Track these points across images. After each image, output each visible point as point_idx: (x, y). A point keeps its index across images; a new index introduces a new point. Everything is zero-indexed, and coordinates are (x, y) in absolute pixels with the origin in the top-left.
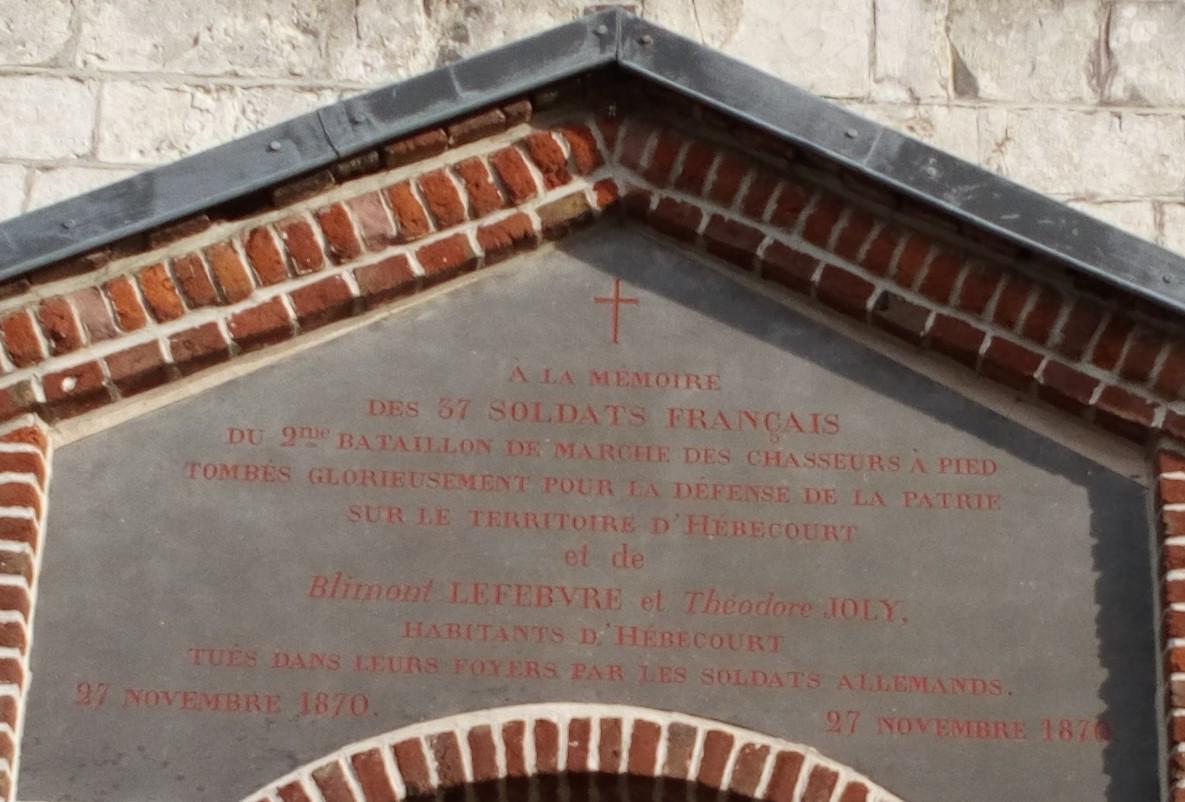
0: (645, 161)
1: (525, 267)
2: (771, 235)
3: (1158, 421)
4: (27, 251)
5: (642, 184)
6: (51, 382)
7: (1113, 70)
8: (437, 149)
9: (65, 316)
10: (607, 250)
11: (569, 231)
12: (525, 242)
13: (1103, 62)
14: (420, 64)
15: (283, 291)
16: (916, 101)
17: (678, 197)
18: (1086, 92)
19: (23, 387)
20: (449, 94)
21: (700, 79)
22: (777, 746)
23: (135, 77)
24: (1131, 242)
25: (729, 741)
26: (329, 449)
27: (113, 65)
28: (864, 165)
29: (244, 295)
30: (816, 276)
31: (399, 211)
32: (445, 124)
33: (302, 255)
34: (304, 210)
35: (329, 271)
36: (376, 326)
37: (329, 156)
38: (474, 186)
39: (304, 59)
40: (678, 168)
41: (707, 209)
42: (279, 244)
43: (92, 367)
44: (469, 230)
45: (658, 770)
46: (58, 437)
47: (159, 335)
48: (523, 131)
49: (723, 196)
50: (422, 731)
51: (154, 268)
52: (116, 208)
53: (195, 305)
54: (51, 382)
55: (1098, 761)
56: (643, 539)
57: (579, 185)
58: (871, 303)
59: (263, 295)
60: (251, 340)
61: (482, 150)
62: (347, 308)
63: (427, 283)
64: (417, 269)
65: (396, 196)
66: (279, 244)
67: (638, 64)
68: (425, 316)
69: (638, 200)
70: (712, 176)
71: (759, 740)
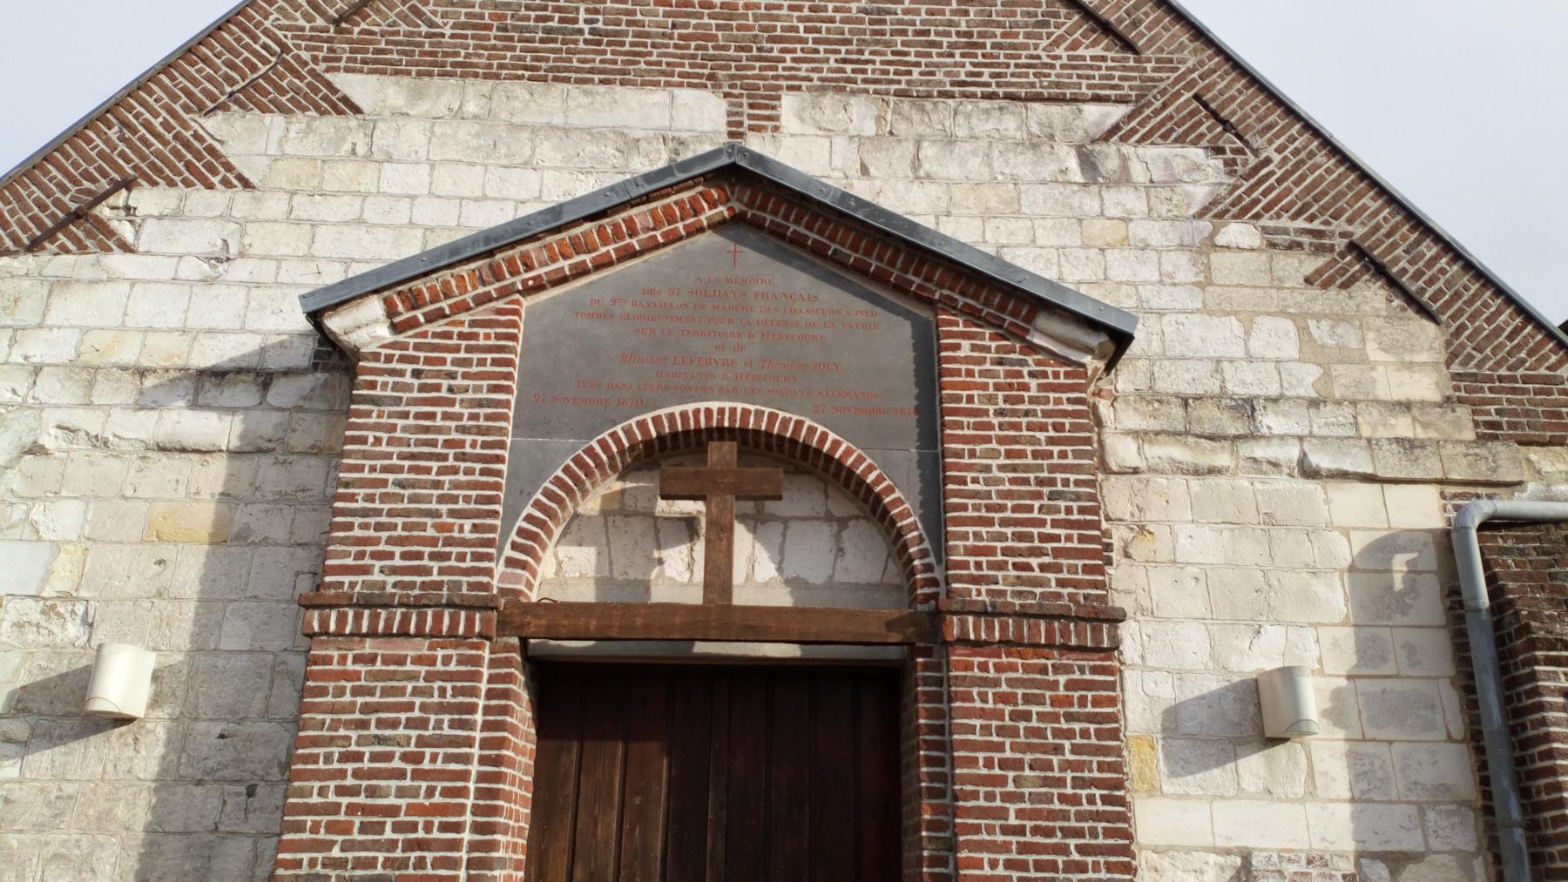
0: (746, 200)
1: (702, 239)
2: (793, 227)
3: (937, 296)
4: (515, 234)
5: (744, 208)
6: (524, 282)
7: (920, 166)
8: (668, 195)
9: (530, 257)
10: (731, 233)
11: (718, 226)
12: (701, 230)
13: (916, 163)
14: (662, 164)
15: (611, 248)
16: (847, 177)
18: (910, 174)
19: (514, 284)
20: (673, 175)
21: (766, 168)
22: (795, 417)
23: (556, 168)
24: (927, 230)
25: (777, 416)
26: (628, 307)
27: (547, 164)
28: (827, 201)
29: (596, 249)
30: (809, 243)
31: (654, 219)
32: (671, 186)
33: (618, 235)
34: (619, 218)
35: (628, 240)
36: (645, 261)
37: (628, 198)
38: (682, 209)
39: (619, 162)
40: (758, 202)
41: (769, 218)
42: (609, 231)
43: (540, 276)
44: (680, 225)
45: (751, 427)
46: (527, 302)
47: (565, 265)
48: (700, 188)
49: (775, 212)
50: (663, 412)
51: (563, 239)
52: (549, 217)
53: (578, 253)
54: (524, 282)
55: (914, 423)
56: (745, 340)
57: (721, 208)
58: (830, 253)
59: (603, 250)
60: (599, 267)
61: (685, 195)
62: (634, 254)
63: (665, 245)
64: (661, 240)
65: (653, 212)
66: (609, 231)
67: (743, 163)
68: (663, 258)
70: (770, 205)
71: (788, 415)
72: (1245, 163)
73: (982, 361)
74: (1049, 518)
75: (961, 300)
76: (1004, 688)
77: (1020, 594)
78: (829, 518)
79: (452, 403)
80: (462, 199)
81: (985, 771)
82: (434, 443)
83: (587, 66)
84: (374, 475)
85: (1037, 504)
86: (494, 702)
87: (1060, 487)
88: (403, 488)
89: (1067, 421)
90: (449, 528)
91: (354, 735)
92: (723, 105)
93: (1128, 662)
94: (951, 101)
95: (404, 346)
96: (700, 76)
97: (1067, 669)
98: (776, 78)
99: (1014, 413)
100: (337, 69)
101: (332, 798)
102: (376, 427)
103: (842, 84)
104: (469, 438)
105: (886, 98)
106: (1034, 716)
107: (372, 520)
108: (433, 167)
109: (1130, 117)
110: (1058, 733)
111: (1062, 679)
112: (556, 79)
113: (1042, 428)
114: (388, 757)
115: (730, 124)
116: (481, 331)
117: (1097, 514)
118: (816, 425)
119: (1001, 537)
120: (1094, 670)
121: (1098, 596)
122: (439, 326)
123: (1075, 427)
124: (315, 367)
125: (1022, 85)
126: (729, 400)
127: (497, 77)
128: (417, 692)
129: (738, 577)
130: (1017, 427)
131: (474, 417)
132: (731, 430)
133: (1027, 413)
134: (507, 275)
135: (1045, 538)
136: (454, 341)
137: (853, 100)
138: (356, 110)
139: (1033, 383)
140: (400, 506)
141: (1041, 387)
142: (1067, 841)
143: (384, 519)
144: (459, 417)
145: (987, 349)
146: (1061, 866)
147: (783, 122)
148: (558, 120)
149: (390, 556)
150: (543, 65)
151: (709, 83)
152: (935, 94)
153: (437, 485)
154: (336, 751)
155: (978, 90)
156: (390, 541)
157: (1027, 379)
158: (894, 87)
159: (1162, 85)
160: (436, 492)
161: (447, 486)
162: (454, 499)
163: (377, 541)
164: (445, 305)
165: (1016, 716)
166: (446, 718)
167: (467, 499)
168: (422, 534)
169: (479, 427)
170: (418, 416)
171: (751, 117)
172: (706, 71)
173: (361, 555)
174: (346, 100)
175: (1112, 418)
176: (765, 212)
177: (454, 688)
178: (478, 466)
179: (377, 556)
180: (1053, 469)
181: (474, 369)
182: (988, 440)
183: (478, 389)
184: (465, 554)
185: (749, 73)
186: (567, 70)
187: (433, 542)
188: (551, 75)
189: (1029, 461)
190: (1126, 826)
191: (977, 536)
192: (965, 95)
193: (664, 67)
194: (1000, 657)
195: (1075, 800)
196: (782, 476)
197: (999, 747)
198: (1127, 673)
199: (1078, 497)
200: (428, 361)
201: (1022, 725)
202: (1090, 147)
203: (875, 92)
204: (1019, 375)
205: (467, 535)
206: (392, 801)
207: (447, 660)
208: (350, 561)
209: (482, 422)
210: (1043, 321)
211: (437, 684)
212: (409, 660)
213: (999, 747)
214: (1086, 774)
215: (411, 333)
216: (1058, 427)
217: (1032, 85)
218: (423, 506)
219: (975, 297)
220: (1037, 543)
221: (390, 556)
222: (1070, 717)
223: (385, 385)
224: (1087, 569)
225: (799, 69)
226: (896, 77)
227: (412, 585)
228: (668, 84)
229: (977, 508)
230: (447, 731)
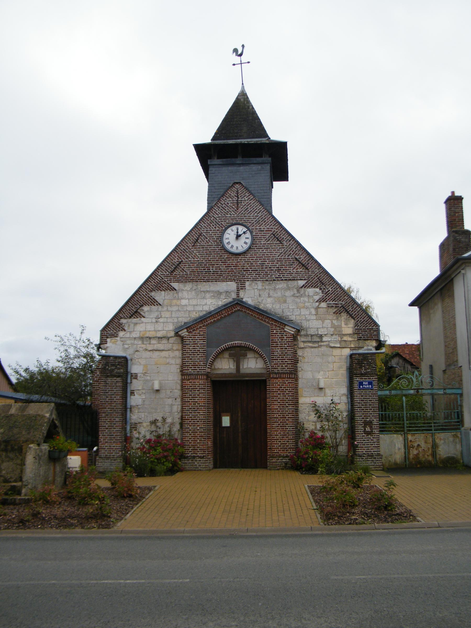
50: (228, 344)
69: (239, 310)
72: (325, 291)
73: (277, 334)
75: (274, 324)
77: (281, 370)
79: (197, 344)
82: (196, 351)
90: (199, 363)
91: (190, 392)
95: (190, 335)
97: (288, 381)
98: (245, 279)
99: (282, 342)
100: (171, 282)
101: (189, 400)
102: (187, 348)
108: (189, 299)
109: (306, 283)
110: (286, 390)
112: (207, 281)
113: (286, 344)
114: (195, 395)
120: (291, 381)
123: (291, 344)
128: (198, 386)
129: (241, 367)
130: (282, 344)
131: (201, 346)
133: (284, 342)
135: (285, 362)
137: (258, 282)
138: (176, 290)
139: (285, 337)
144: (198, 346)
145: (278, 331)
147: (246, 287)
148: (208, 290)
153: (197, 357)
154: (188, 394)
156: (191, 365)
158: (265, 279)
159: (312, 276)
162: (199, 359)
163: (190, 366)
165: (280, 387)
167: (201, 359)
170: (193, 346)
171: (241, 287)
172: (233, 278)
173: (188, 368)
174: (173, 288)
180: (287, 351)
182: (278, 346)
183: (201, 342)
187: (197, 365)
191: (276, 362)
192: (277, 280)
195: (287, 398)
205: (202, 364)
206: (196, 401)
207: (201, 382)
208: (186, 369)
210: (286, 327)
213: (278, 392)
216: (289, 344)
217: (289, 277)
221: (192, 368)
222: (288, 387)
227: (195, 372)
228: (226, 281)
229: (276, 357)
230: (202, 392)
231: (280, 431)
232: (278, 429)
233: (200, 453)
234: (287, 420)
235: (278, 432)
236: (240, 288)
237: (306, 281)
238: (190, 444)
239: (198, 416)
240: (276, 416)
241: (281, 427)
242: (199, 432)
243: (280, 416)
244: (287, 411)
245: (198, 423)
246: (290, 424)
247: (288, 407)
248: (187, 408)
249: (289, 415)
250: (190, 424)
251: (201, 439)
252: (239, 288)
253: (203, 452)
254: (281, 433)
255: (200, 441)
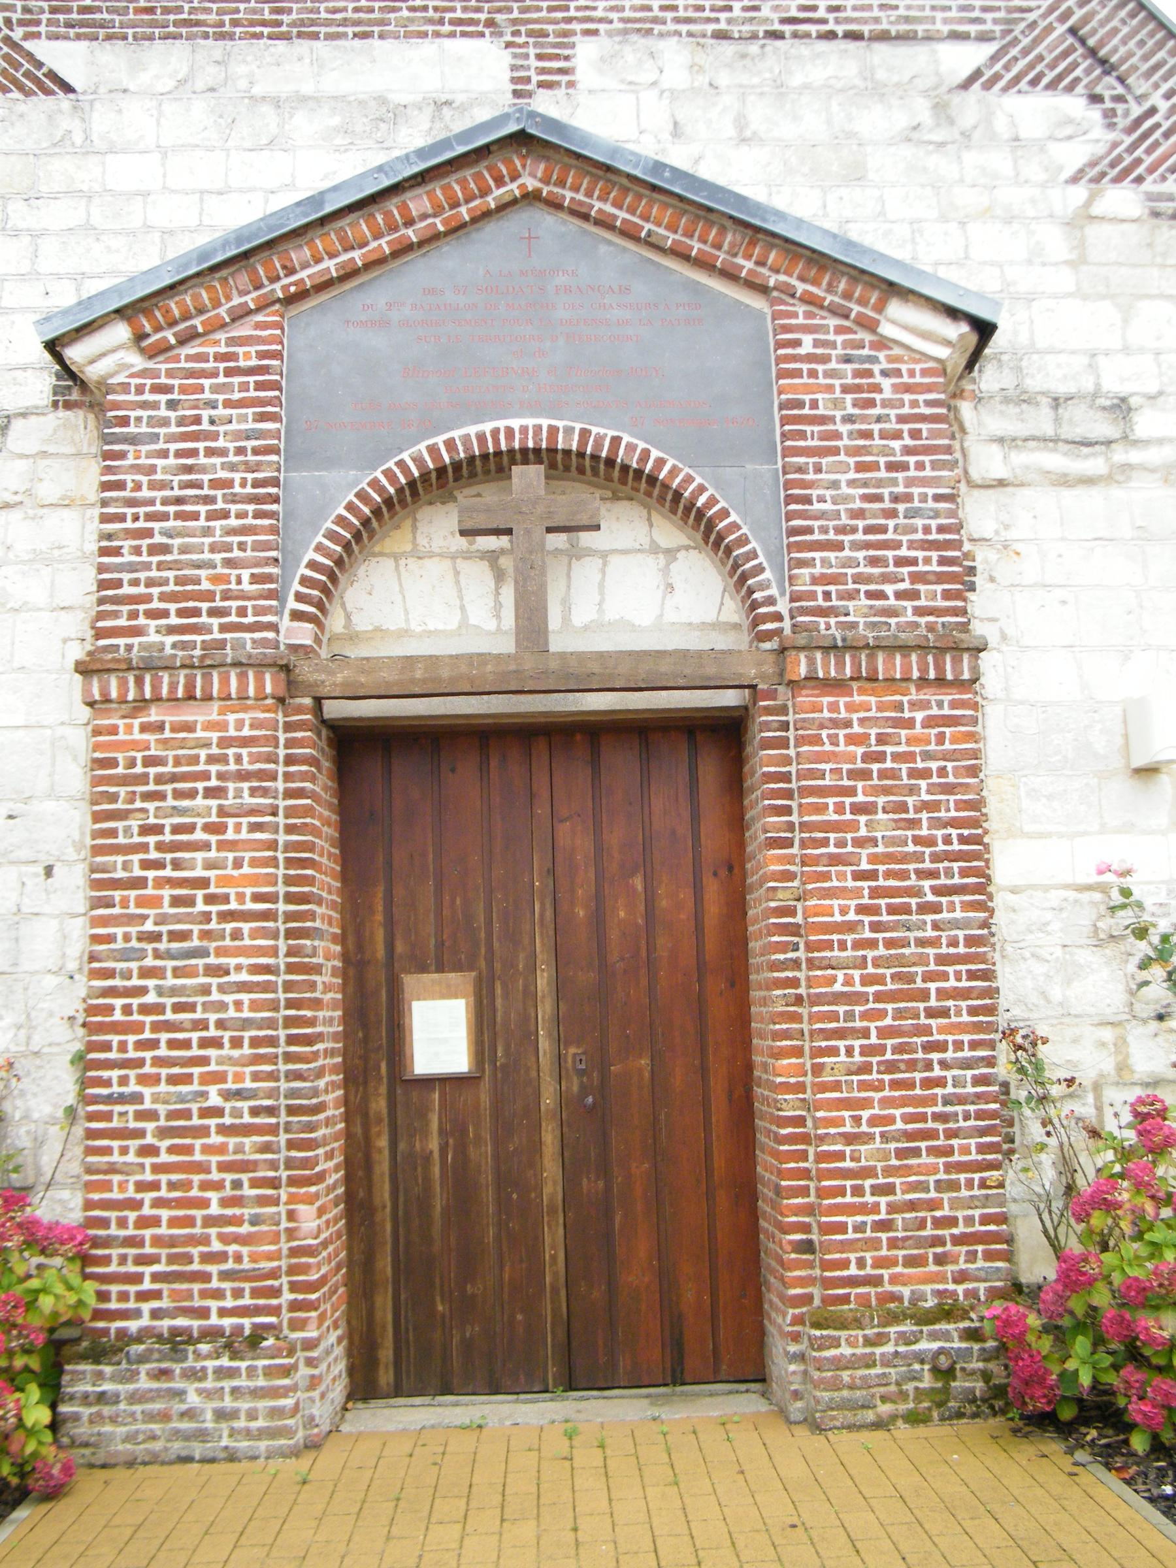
0: (539, 175)
2: (598, 205)
3: (771, 283)
4: (271, 230)
5: (539, 185)
6: (285, 288)
17: (556, 190)
19: (273, 291)
25: (590, 432)
28: (638, 173)
30: (618, 224)
40: (555, 177)
41: (569, 195)
43: (302, 280)
44: (463, 210)
49: (576, 189)
50: (456, 434)
53: (346, 250)
58: (643, 235)
59: (374, 245)
70: (570, 180)
71: (602, 431)
72: (1127, 113)
73: (825, 359)
74: (905, 538)
75: (801, 287)
76: (857, 729)
78: (655, 549)
79: (214, 436)
80: (202, 192)
81: (836, 817)
83: (338, 16)
84: (138, 525)
85: (891, 523)
86: (292, 769)
87: (916, 504)
88: (171, 537)
89: (924, 427)
90: (225, 579)
91: (151, 806)
92: (505, 58)
93: (990, 697)
94: (779, 43)
96: (475, 22)
97: (924, 705)
98: (569, 20)
99: (864, 419)
101: (138, 872)
102: (137, 469)
103: (648, 26)
104: (237, 477)
105: (702, 41)
106: (889, 758)
107: (142, 576)
109: (994, 58)
110: (914, 774)
111: (919, 716)
112: (300, 35)
113: (897, 435)
114: (191, 828)
115: (514, 81)
116: (241, 350)
117: (958, 532)
118: (635, 441)
119: (850, 563)
120: (954, 705)
121: (958, 623)
122: (192, 349)
123: (934, 434)
124: (55, 404)
125: (865, 21)
126: (532, 416)
127: (231, 36)
128: (211, 759)
129: (554, 621)
130: (867, 435)
132: (537, 451)
133: (879, 419)
134: (266, 282)
135: (901, 562)
136: (211, 365)
139: (886, 383)
140: (168, 558)
141: (896, 388)
142: (921, 883)
143: (154, 574)
144: (223, 452)
145: (833, 345)
146: (914, 907)
147: (578, 76)
148: (307, 88)
149: (165, 614)
150: (285, 18)
151: (487, 31)
152: (761, 34)
153: (207, 532)
155: (813, 29)
156: (163, 597)
157: (878, 379)
159: (1031, 17)
160: (207, 540)
161: (218, 532)
163: (148, 599)
164: (197, 322)
166: (246, 785)
168: (196, 587)
169: (246, 463)
170: (179, 454)
171: (542, 71)
172: (483, 16)
175: (975, 421)
176: (564, 187)
177: (250, 754)
178: (250, 508)
179: (151, 614)
180: (910, 482)
181: (237, 396)
182: (835, 451)
183: (243, 419)
184: (246, 608)
185: (535, 16)
186: (313, 23)
187: (209, 596)
188: (295, 30)
189: (883, 474)
190: (982, 864)
192: (795, 35)
193: (431, 13)
194: (852, 695)
195: (930, 842)
196: (598, 502)
197: (852, 792)
198: (988, 709)
199: (937, 514)
200: (183, 390)
201: (875, 767)
202: (946, 97)
203: (690, 34)
204: (869, 374)
205: (246, 586)
206: (199, 873)
208: (123, 622)
209: (250, 458)
210: (896, 309)
211: (231, 752)
212: (199, 727)
213: (852, 792)
214: (942, 814)
215: (161, 358)
216: (916, 434)
217: (877, 20)
218: (194, 557)
219: (816, 282)
220: (891, 568)
221: (165, 614)
222: (927, 756)
223: (139, 419)
224: (947, 595)
225: (595, 8)
226: (713, 15)
228: (437, 34)
231: (886, 1102)
232: (863, 1085)
233: (229, 1303)
234: (931, 1013)
235: (865, 1114)
236: (535, 78)
237: (991, 48)
238: (148, 1233)
239: (215, 996)
240: (848, 981)
241: (891, 1067)
242: (223, 1130)
243: (879, 980)
244: (934, 942)
245: (212, 1053)
246: (959, 1045)
247: (936, 908)
248: (119, 931)
249: (944, 976)
250: (148, 1069)
251: (237, 1185)
252: (528, 80)
253: (256, 1293)
254: (891, 1120)
255: (225, 1202)
